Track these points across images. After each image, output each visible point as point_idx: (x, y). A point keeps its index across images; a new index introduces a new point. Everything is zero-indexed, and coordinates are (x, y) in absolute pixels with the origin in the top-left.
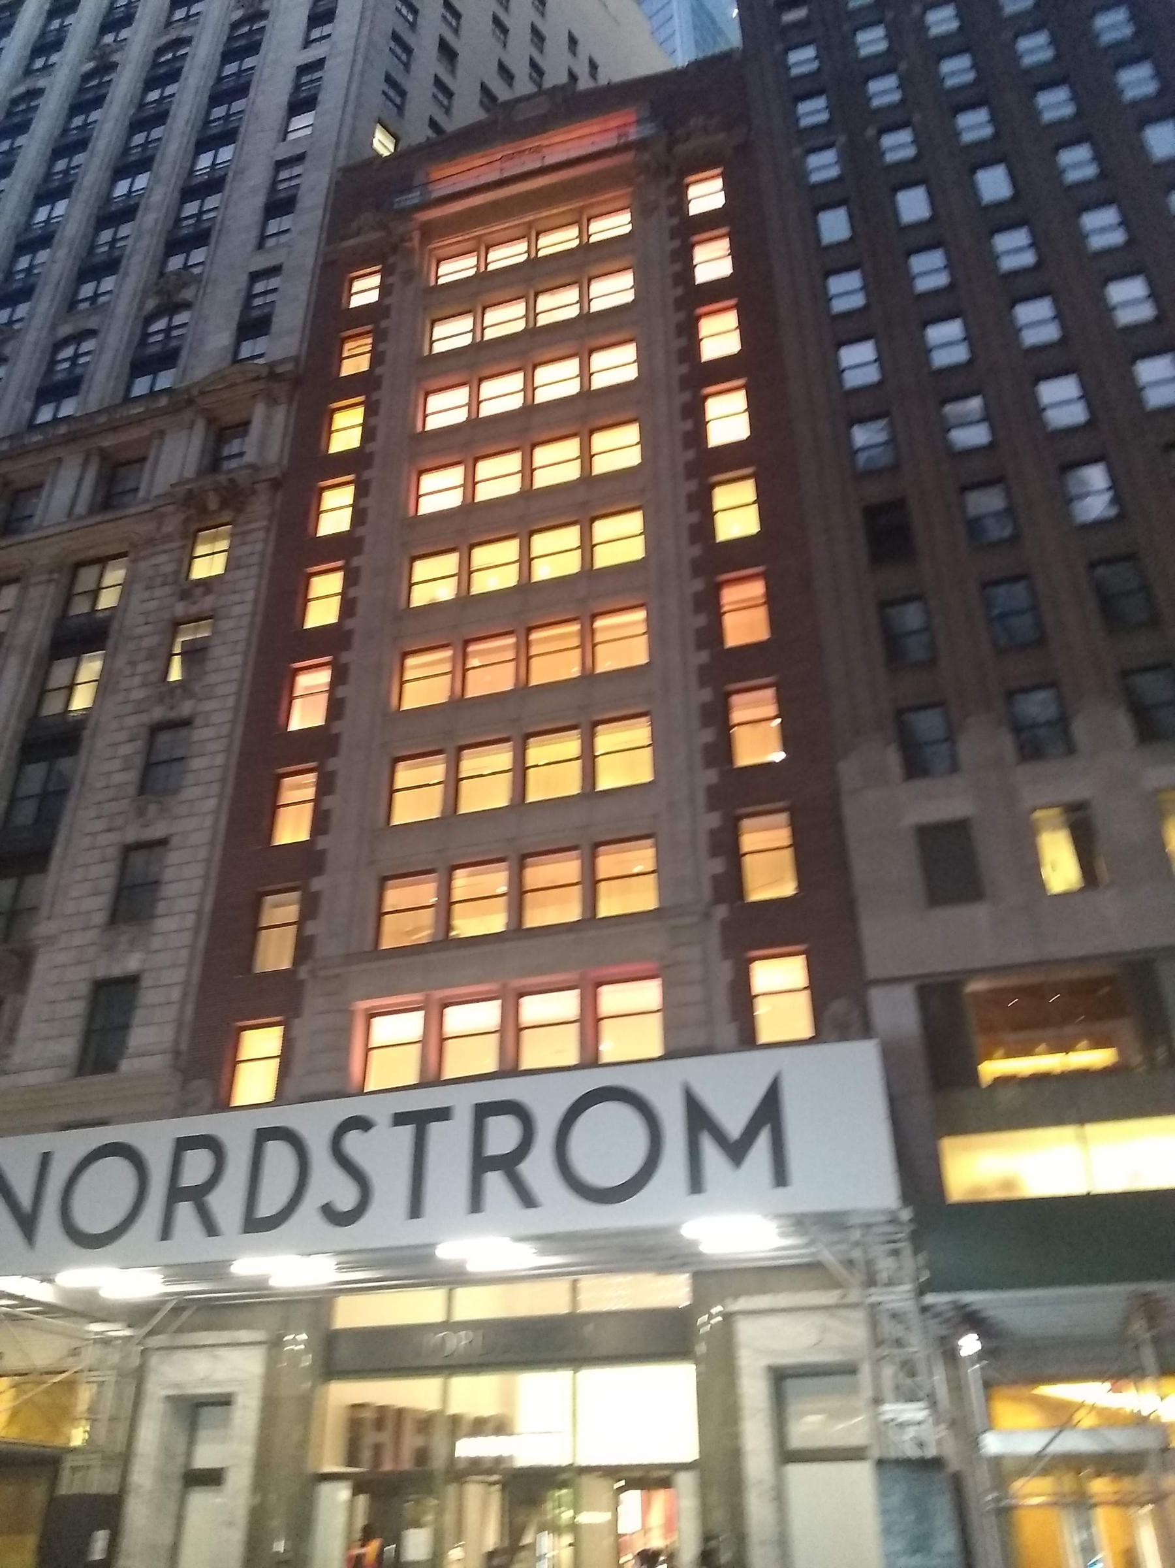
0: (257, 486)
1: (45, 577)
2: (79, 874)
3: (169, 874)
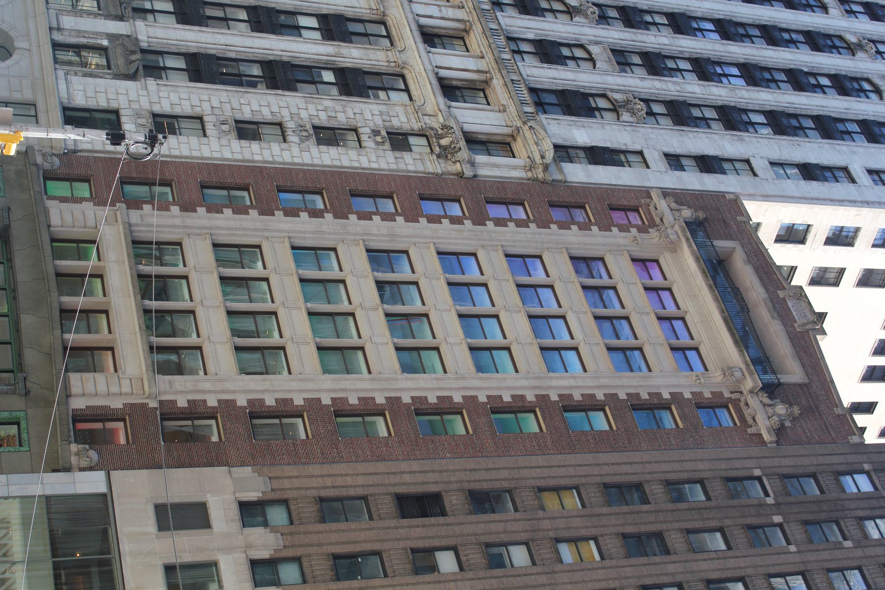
0: (458, 164)
2: (184, 96)
3: (182, 139)
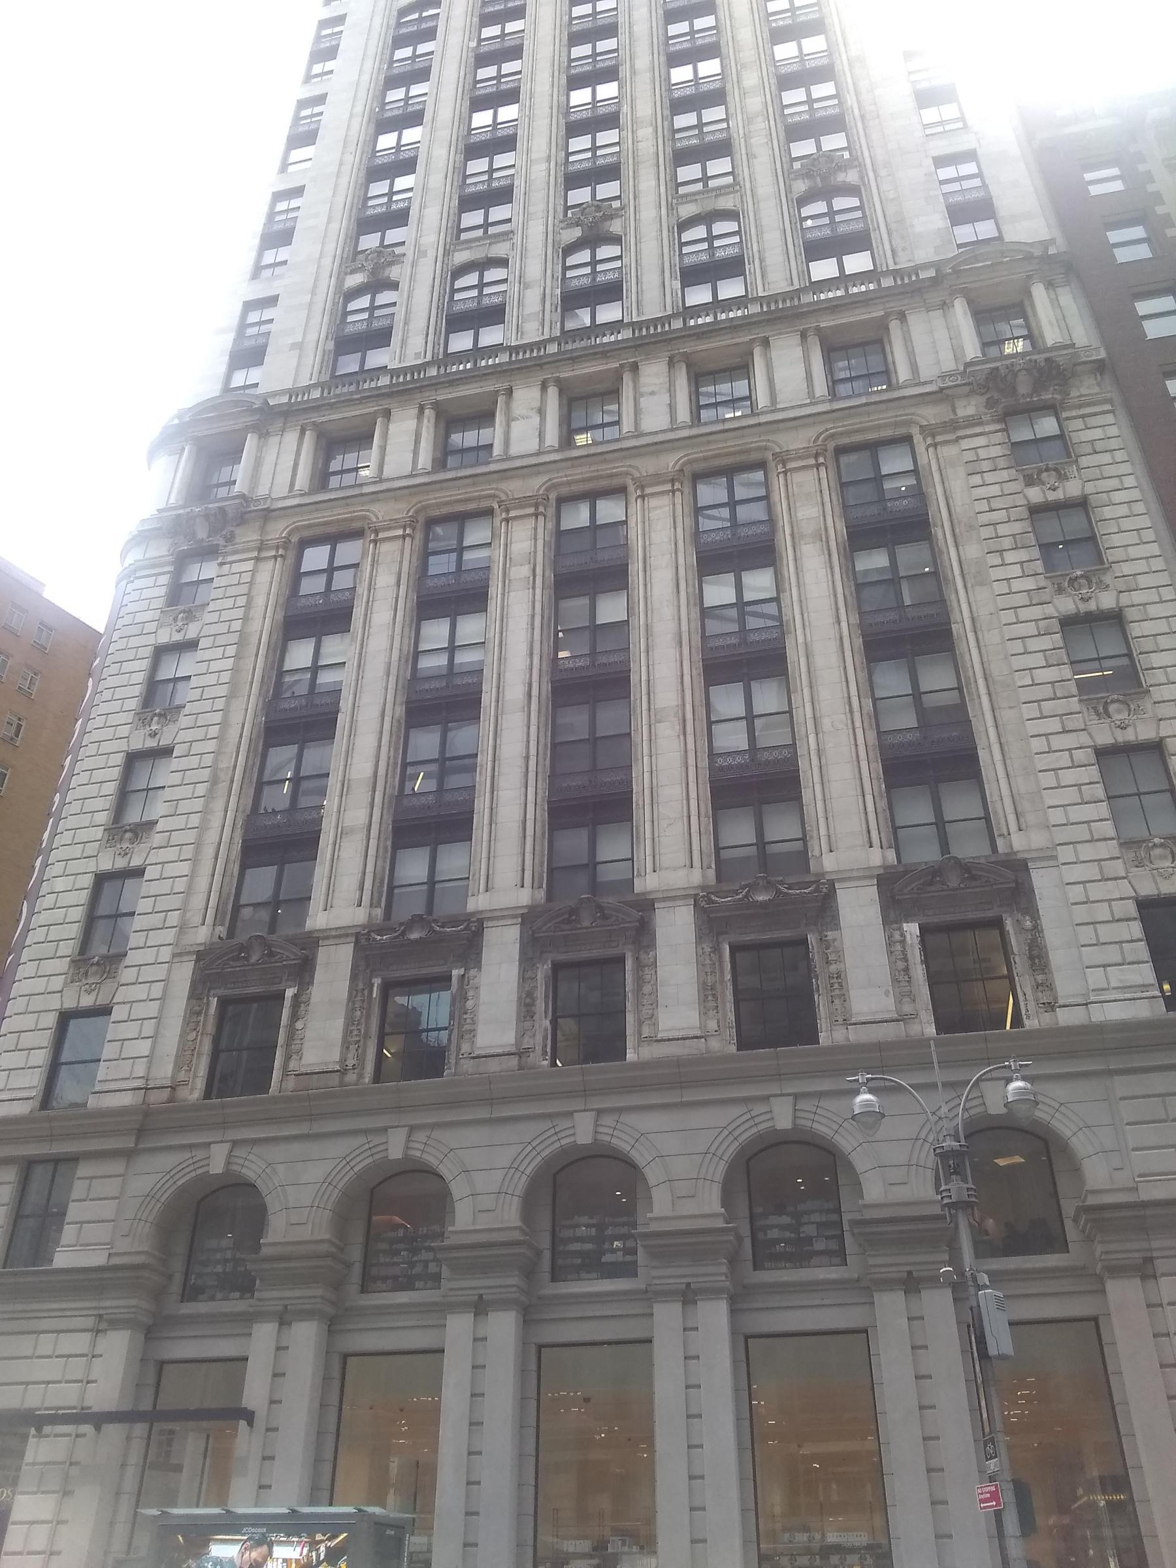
0: (1079, 368)
1: (812, 461)
